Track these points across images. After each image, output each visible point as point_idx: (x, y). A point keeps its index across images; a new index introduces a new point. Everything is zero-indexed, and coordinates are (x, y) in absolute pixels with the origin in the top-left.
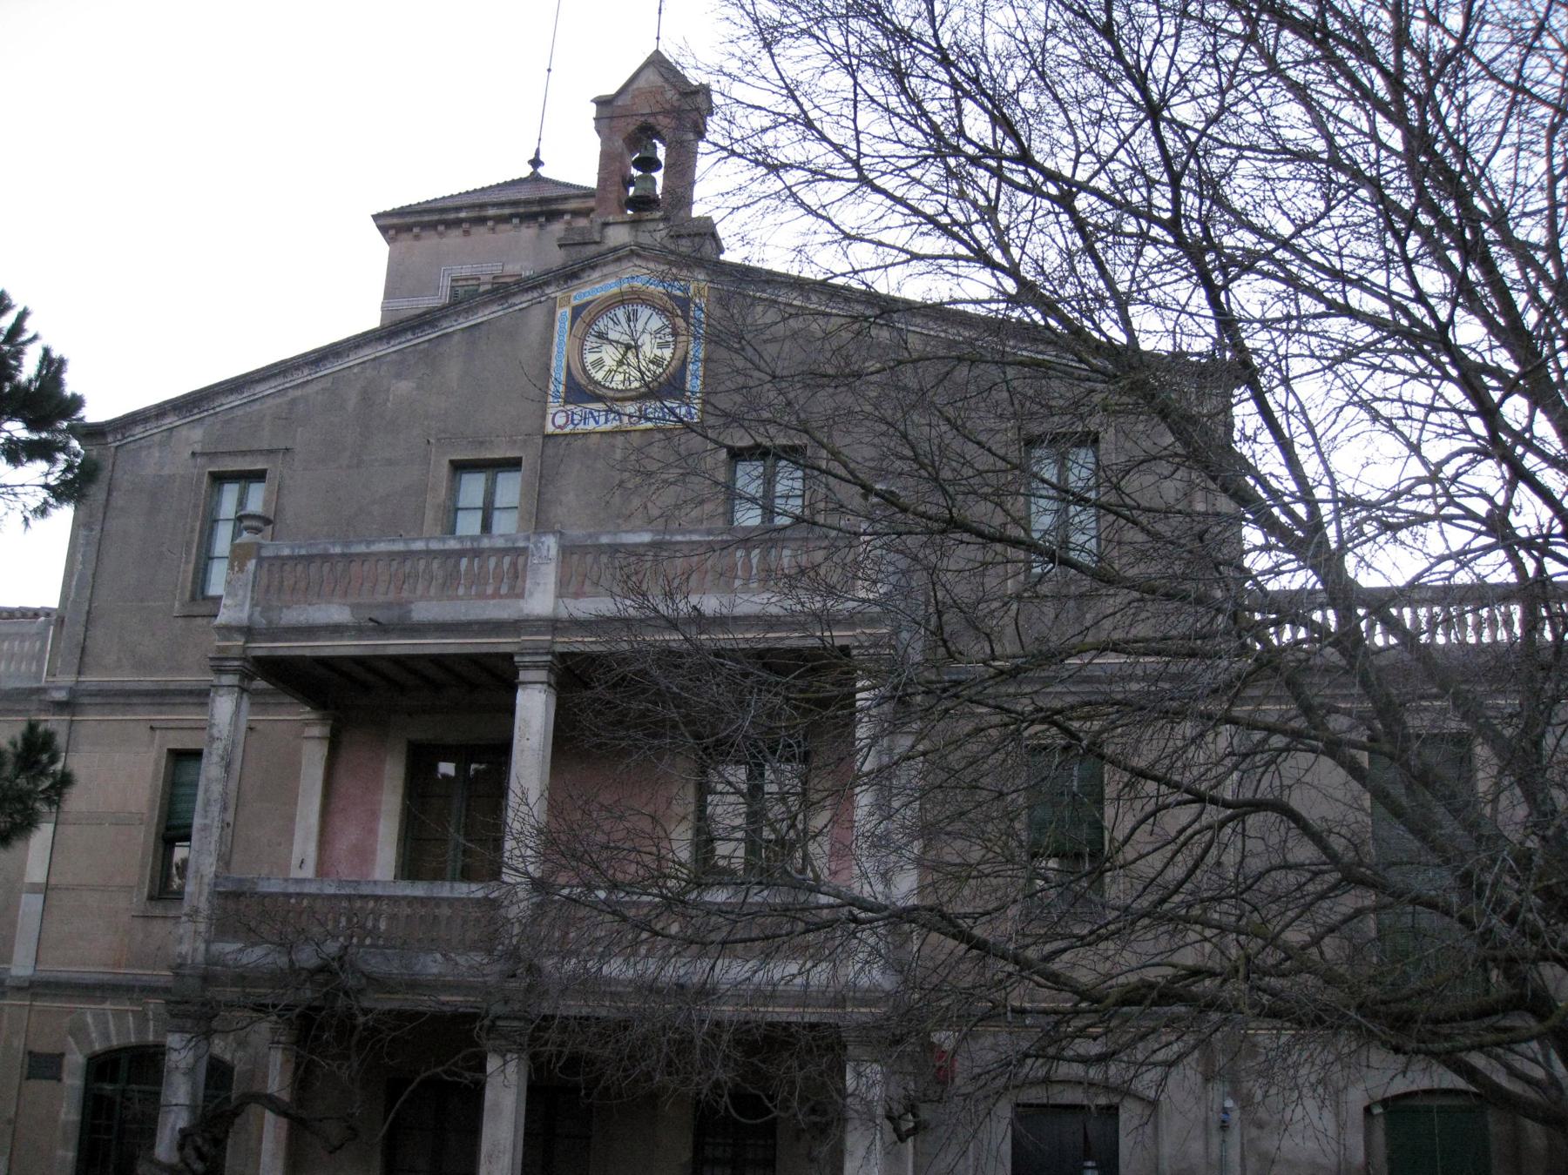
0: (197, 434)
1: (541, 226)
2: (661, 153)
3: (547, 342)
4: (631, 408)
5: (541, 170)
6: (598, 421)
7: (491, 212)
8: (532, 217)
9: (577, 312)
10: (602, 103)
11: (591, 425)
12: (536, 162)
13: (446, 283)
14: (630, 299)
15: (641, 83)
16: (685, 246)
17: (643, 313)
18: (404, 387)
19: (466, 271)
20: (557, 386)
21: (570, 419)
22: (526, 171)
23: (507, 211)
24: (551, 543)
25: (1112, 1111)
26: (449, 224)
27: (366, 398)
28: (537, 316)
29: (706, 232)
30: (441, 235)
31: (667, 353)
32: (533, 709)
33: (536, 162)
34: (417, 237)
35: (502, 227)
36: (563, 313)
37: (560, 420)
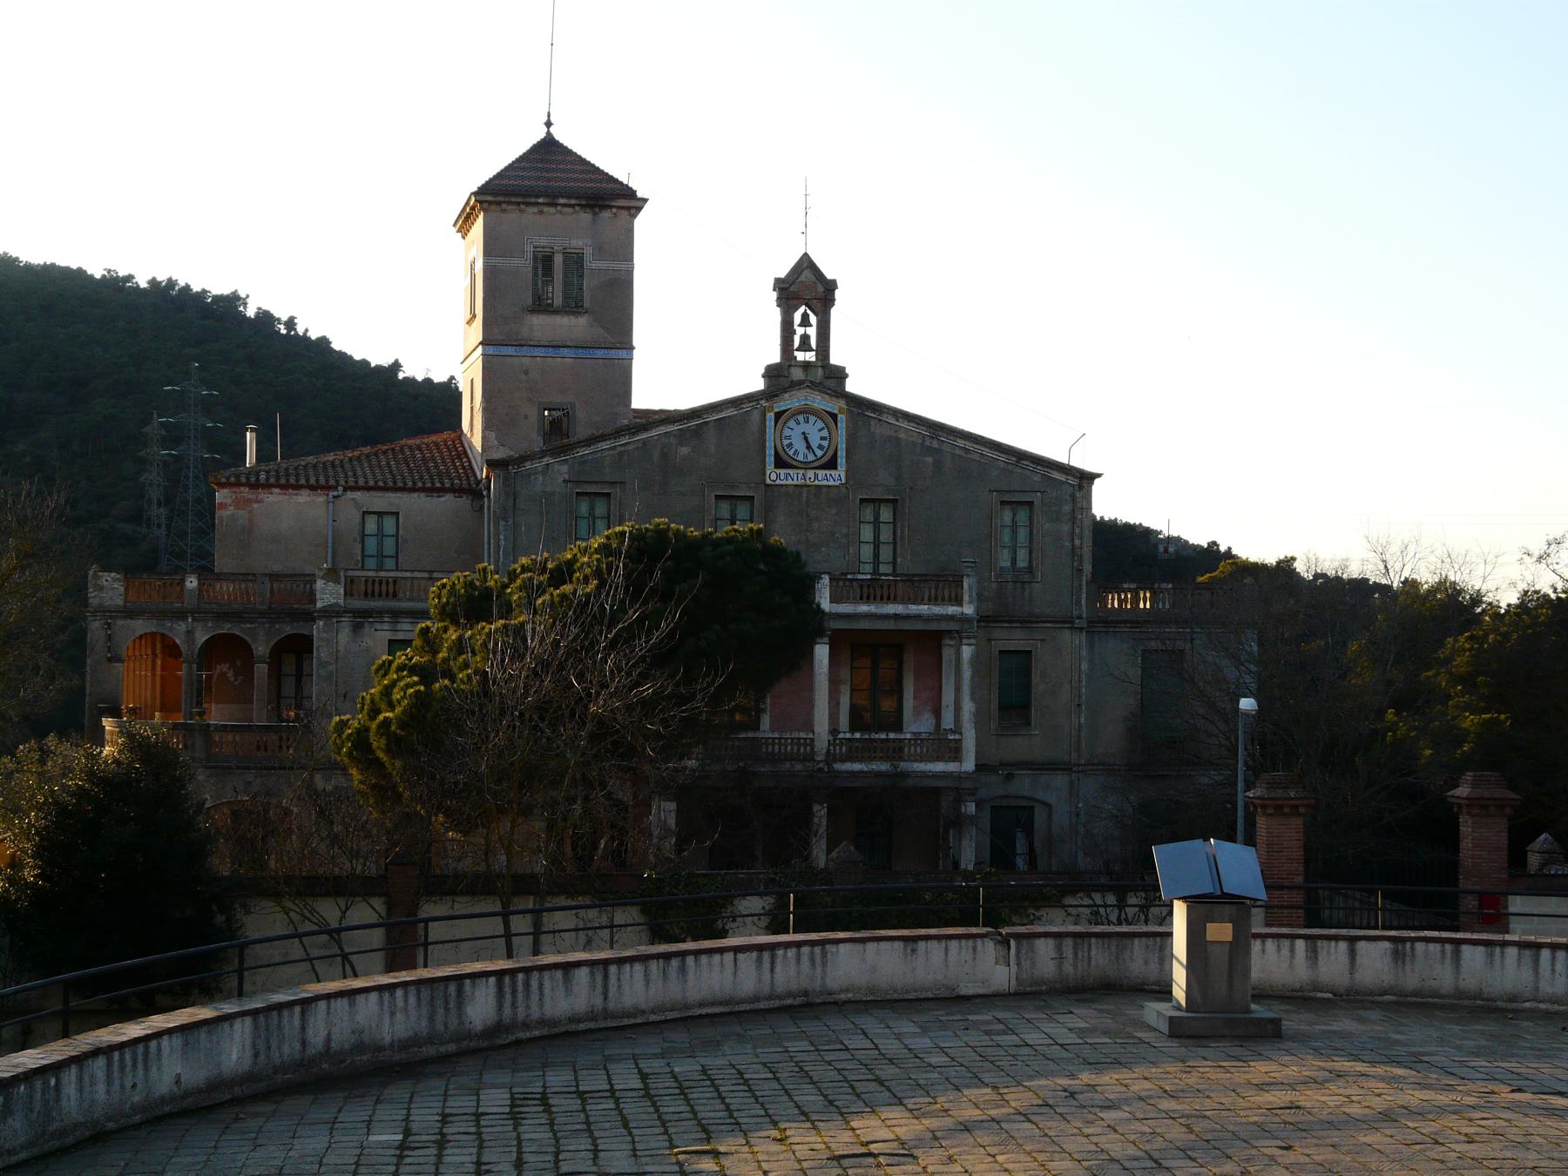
0: (565, 468)
1: (595, 214)
2: (813, 319)
3: (763, 431)
4: (810, 474)
5: (552, 129)
6: (792, 478)
7: (562, 201)
8: (591, 207)
9: (778, 415)
10: (778, 281)
11: (790, 482)
12: (549, 124)
13: (529, 249)
14: (807, 411)
15: (802, 278)
16: (831, 383)
17: (812, 419)
18: (685, 450)
19: (543, 242)
20: (770, 459)
21: (778, 476)
22: (540, 134)
23: (573, 202)
24: (826, 579)
25: (1032, 808)
26: (527, 204)
27: (664, 455)
28: (756, 416)
29: (840, 375)
30: (522, 211)
31: (825, 443)
32: (822, 652)
33: (549, 124)
34: (504, 211)
35: (567, 210)
36: (770, 416)
37: (773, 476)
